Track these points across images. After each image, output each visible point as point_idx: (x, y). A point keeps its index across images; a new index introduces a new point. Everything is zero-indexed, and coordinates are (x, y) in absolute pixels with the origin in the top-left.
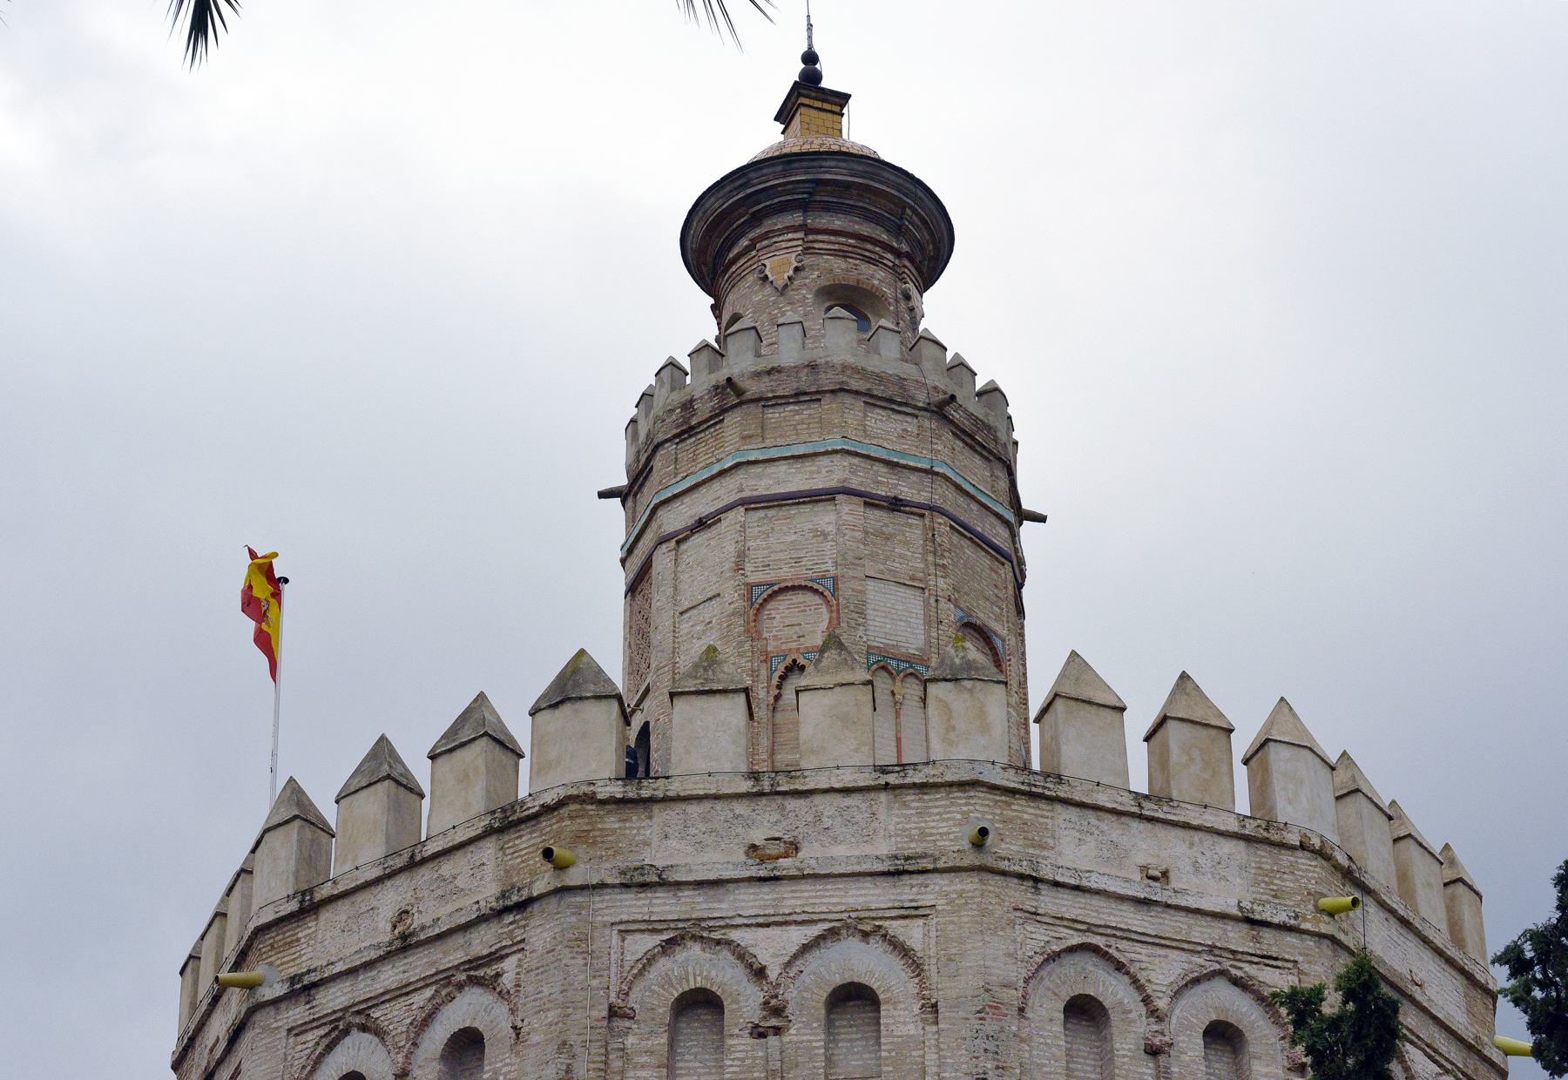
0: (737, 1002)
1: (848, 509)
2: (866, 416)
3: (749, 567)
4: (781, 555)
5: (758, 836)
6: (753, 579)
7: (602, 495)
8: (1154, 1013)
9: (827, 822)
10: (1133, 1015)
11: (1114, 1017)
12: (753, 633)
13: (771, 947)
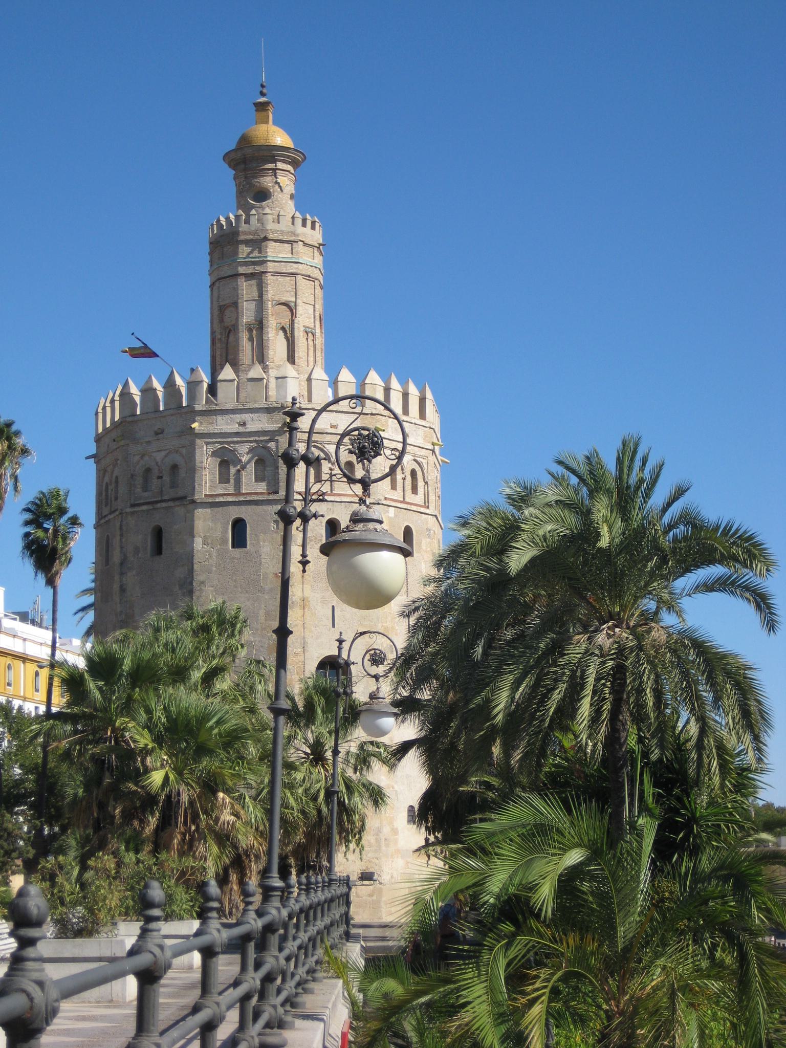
5: (156, 429)
6: (222, 304)
12: (221, 321)
13: (159, 456)
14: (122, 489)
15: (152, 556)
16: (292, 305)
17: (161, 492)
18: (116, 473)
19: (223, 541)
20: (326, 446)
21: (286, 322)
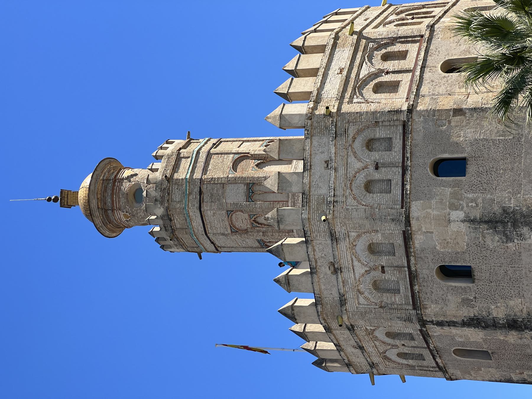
0: (375, 277)
1: (205, 207)
2: (175, 201)
3: (226, 233)
4: (222, 224)
5: (329, 272)
7: (201, 258)
8: (366, 167)
9: (323, 255)
10: (368, 172)
11: (369, 178)
12: (246, 231)
13: (360, 270)
14: (398, 326)
15: (474, 282)
16: (237, 156)
17: (399, 267)
18: (380, 334)
19: (457, 185)
20: (361, 77)
21: (252, 163)
